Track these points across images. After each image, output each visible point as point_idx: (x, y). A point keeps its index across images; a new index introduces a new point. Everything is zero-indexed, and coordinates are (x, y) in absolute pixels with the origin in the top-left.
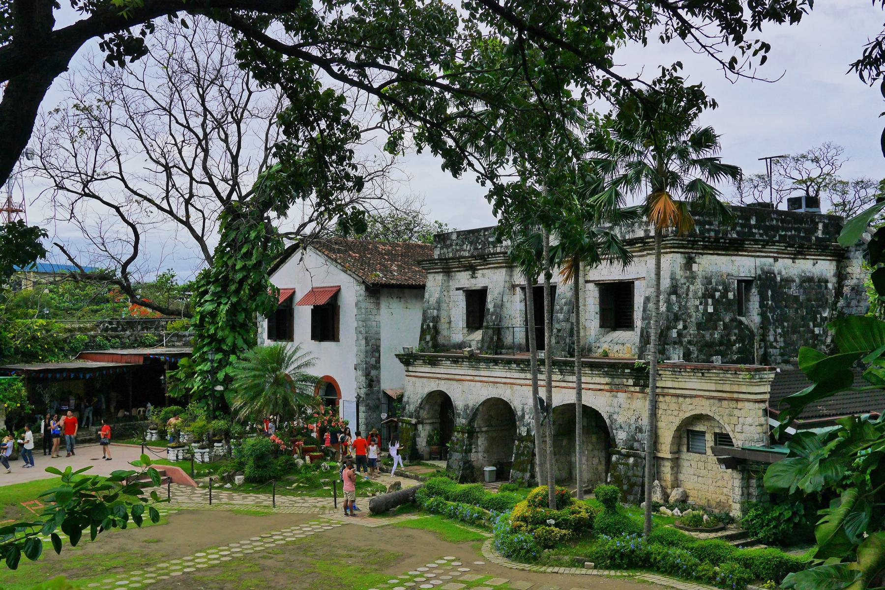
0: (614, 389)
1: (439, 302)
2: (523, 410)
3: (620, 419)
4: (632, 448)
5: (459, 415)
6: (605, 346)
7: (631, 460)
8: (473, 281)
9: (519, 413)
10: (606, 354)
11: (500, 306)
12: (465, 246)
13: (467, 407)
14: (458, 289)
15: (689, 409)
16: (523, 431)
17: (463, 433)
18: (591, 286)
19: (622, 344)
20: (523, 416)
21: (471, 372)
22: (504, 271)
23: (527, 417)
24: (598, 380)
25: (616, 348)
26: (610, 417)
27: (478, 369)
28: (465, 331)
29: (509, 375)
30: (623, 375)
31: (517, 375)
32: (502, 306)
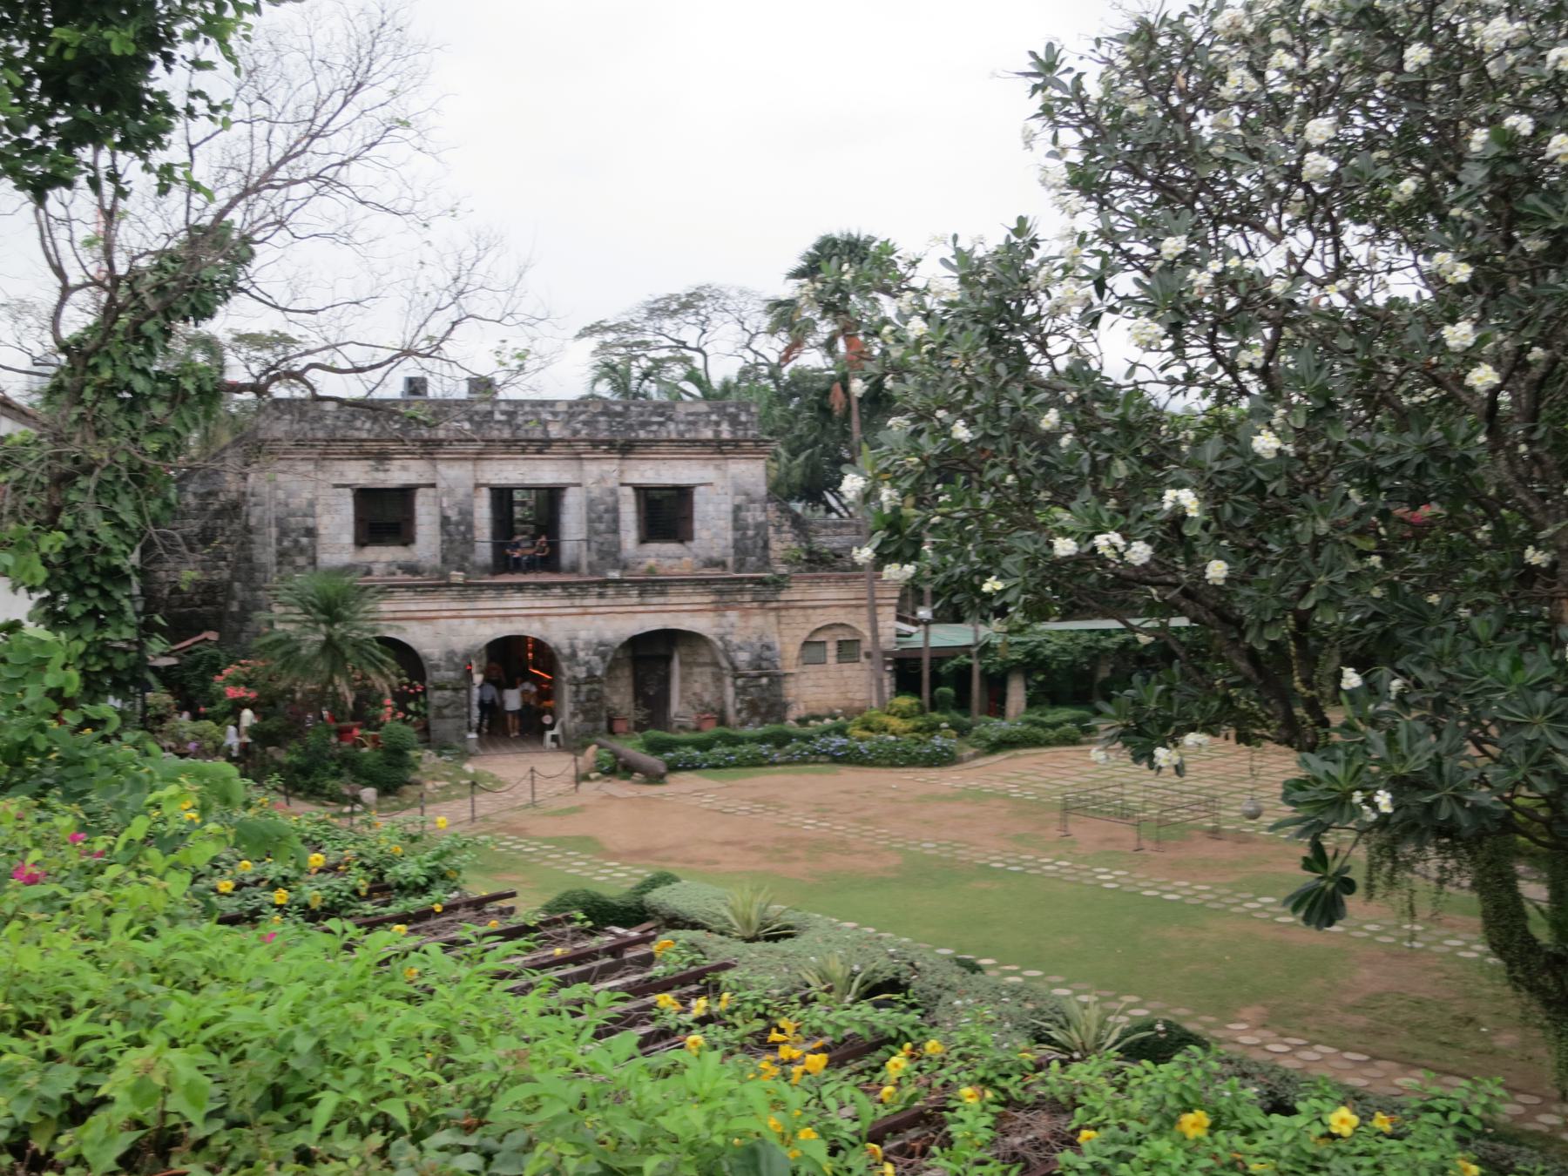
0: (719, 608)
1: (312, 504)
2: (572, 646)
3: (736, 640)
4: (759, 667)
5: (437, 667)
6: (652, 561)
7: (764, 681)
8: (381, 475)
9: (566, 651)
10: (651, 571)
11: (467, 515)
12: (358, 424)
13: (450, 655)
14: (337, 486)
15: (820, 619)
16: (581, 673)
17: (455, 690)
18: (629, 491)
19: (663, 556)
20: (574, 655)
21: (454, 605)
22: (469, 466)
23: (581, 654)
24: (698, 599)
25: (669, 562)
26: (722, 638)
27: (476, 599)
28: (352, 549)
29: (538, 603)
30: (741, 591)
31: (552, 603)
32: (471, 514)
